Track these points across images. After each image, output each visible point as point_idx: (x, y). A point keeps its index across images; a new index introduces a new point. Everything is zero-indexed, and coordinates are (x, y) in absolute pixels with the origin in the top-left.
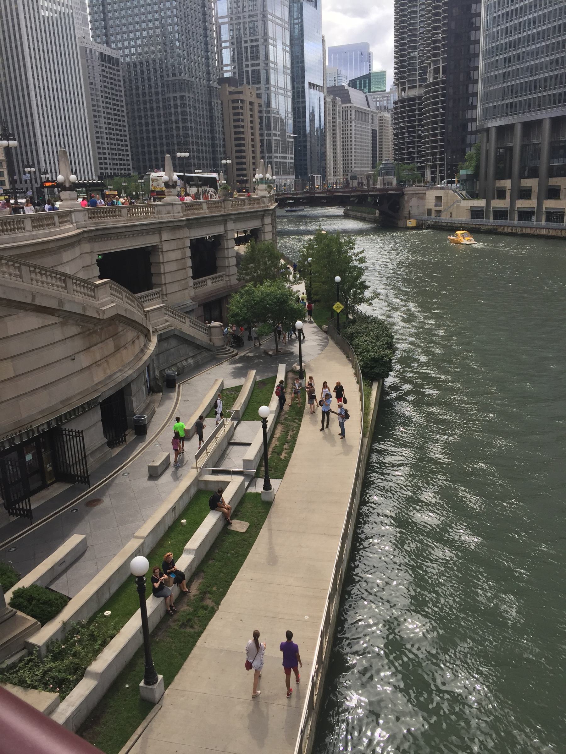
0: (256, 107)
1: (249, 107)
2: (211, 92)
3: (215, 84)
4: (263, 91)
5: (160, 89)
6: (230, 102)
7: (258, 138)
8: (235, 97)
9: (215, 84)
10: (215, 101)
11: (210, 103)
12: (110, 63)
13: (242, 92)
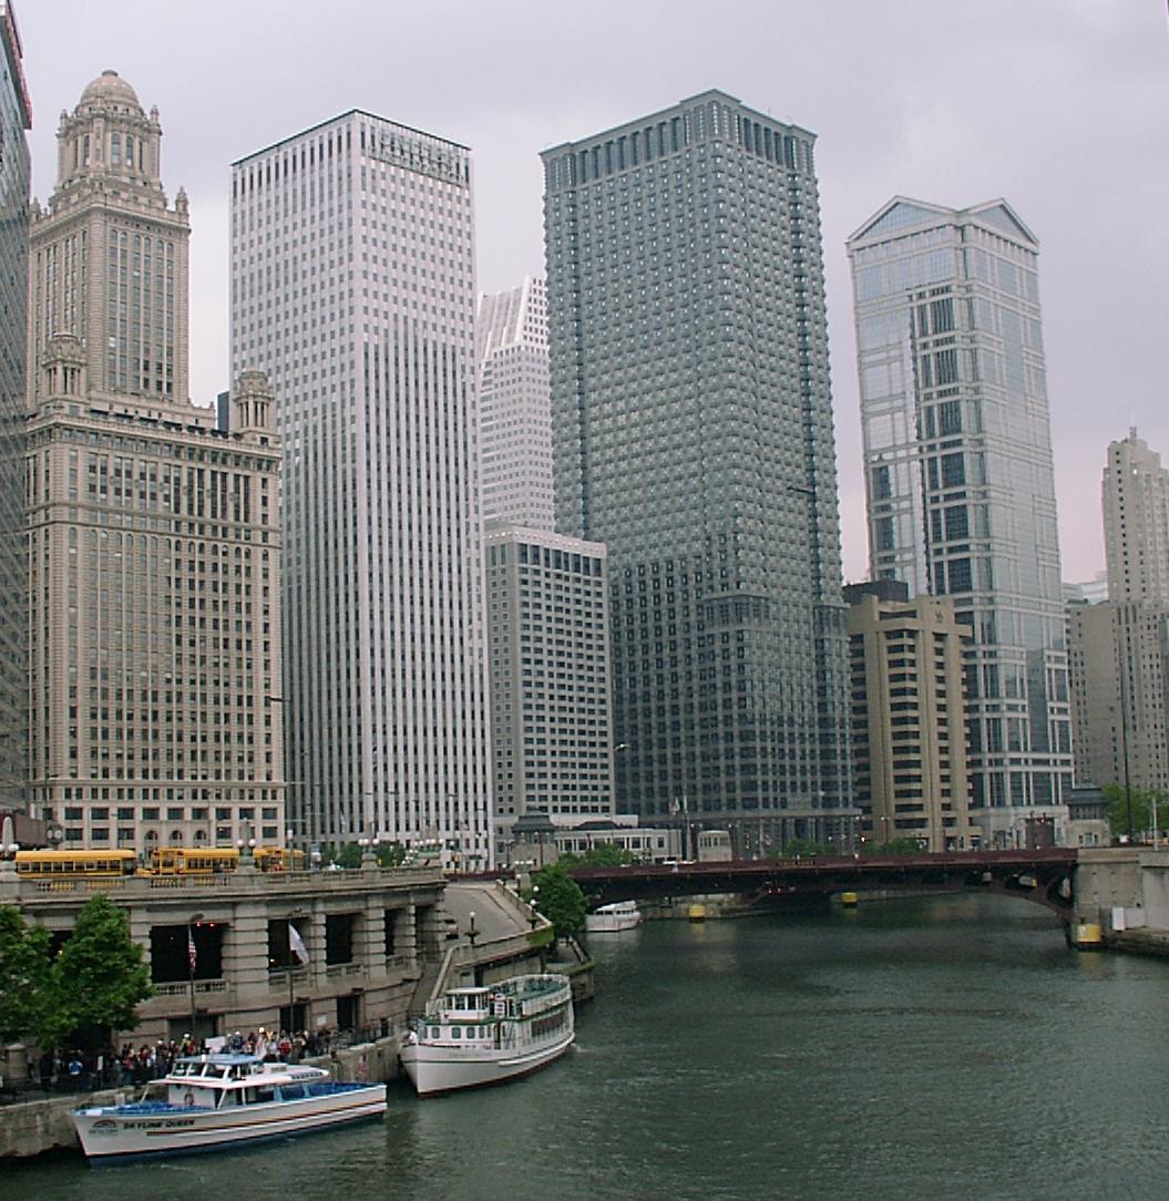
0: (954, 647)
1: (933, 644)
2: (822, 616)
3: (837, 601)
4: (977, 608)
5: (693, 618)
6: (882, 636)
7: (958, 717)
8: (896, 624)
9: (837, 601)
10: (833, 637)
11: (819, 643)
12: (577, 570)
13: (912, 614)
